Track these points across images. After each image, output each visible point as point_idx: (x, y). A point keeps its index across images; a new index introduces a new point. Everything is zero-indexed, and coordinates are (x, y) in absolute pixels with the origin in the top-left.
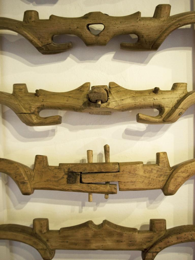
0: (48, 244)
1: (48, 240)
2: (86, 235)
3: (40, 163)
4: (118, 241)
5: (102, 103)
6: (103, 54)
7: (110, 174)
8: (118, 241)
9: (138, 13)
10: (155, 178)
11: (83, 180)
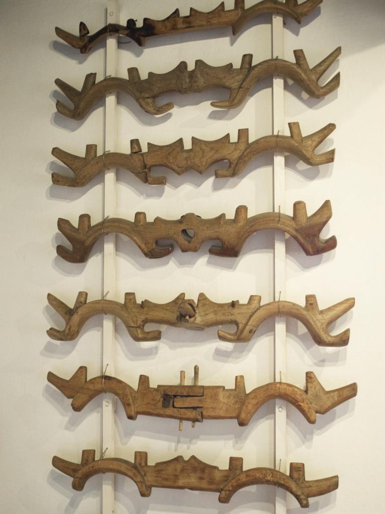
0: (146, 478)
1: (145, 475)
2: (176, 470)
5: (190, 317)
7: (196, 398)
9: (223, 215)
10: (231, 405)
11: (176, 405)
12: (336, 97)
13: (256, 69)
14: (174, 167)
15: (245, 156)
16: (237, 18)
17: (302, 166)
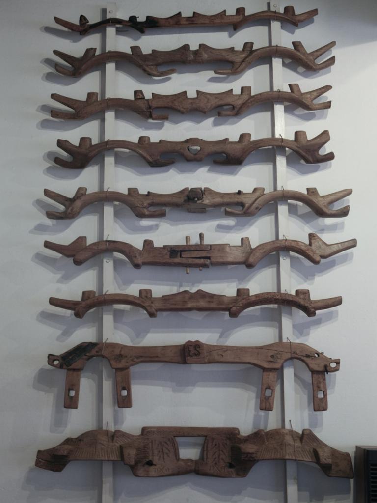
3: (148, 245)
4: (209, 302)
5: (198, 200)
6: (199, 168)
8: (209, 302)
9: (226, 139)
11: (183, 256)
12: (330, 71)
13: (255, 53)
14: (179, 108)
15: (249, 103)
16: (238, 20)
17: (301, 111)
